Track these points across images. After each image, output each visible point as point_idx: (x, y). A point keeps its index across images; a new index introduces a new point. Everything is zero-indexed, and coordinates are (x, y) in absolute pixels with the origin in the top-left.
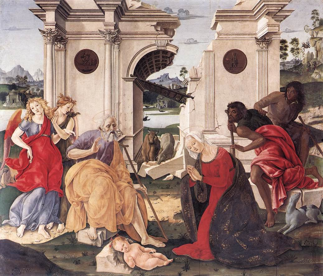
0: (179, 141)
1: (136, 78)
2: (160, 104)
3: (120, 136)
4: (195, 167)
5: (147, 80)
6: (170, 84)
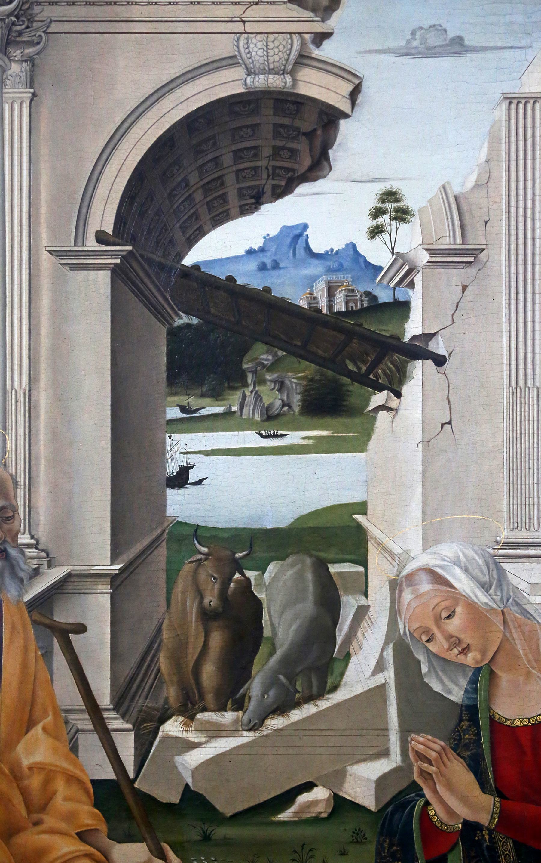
0: (363, 601)
1: (130, 252)
2: (258, 397)
3: (36, 572)
4: (454, 750)
5: (188, 260)
6: (313, 279)
